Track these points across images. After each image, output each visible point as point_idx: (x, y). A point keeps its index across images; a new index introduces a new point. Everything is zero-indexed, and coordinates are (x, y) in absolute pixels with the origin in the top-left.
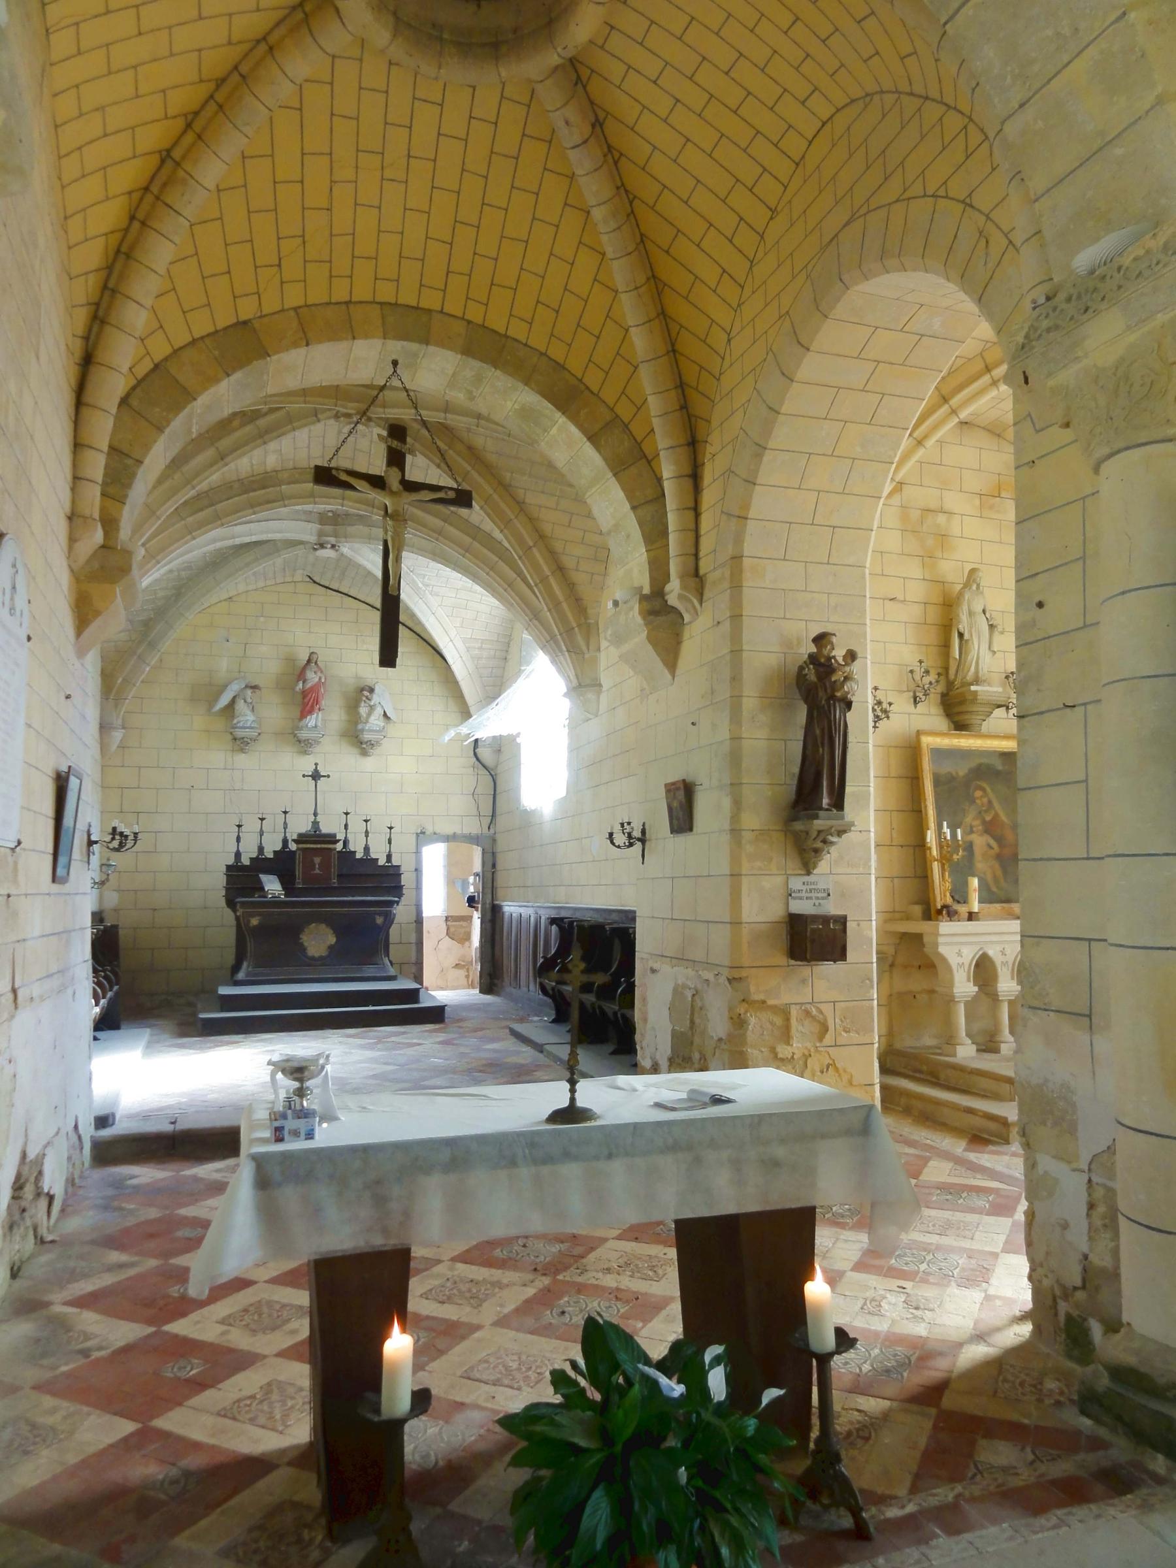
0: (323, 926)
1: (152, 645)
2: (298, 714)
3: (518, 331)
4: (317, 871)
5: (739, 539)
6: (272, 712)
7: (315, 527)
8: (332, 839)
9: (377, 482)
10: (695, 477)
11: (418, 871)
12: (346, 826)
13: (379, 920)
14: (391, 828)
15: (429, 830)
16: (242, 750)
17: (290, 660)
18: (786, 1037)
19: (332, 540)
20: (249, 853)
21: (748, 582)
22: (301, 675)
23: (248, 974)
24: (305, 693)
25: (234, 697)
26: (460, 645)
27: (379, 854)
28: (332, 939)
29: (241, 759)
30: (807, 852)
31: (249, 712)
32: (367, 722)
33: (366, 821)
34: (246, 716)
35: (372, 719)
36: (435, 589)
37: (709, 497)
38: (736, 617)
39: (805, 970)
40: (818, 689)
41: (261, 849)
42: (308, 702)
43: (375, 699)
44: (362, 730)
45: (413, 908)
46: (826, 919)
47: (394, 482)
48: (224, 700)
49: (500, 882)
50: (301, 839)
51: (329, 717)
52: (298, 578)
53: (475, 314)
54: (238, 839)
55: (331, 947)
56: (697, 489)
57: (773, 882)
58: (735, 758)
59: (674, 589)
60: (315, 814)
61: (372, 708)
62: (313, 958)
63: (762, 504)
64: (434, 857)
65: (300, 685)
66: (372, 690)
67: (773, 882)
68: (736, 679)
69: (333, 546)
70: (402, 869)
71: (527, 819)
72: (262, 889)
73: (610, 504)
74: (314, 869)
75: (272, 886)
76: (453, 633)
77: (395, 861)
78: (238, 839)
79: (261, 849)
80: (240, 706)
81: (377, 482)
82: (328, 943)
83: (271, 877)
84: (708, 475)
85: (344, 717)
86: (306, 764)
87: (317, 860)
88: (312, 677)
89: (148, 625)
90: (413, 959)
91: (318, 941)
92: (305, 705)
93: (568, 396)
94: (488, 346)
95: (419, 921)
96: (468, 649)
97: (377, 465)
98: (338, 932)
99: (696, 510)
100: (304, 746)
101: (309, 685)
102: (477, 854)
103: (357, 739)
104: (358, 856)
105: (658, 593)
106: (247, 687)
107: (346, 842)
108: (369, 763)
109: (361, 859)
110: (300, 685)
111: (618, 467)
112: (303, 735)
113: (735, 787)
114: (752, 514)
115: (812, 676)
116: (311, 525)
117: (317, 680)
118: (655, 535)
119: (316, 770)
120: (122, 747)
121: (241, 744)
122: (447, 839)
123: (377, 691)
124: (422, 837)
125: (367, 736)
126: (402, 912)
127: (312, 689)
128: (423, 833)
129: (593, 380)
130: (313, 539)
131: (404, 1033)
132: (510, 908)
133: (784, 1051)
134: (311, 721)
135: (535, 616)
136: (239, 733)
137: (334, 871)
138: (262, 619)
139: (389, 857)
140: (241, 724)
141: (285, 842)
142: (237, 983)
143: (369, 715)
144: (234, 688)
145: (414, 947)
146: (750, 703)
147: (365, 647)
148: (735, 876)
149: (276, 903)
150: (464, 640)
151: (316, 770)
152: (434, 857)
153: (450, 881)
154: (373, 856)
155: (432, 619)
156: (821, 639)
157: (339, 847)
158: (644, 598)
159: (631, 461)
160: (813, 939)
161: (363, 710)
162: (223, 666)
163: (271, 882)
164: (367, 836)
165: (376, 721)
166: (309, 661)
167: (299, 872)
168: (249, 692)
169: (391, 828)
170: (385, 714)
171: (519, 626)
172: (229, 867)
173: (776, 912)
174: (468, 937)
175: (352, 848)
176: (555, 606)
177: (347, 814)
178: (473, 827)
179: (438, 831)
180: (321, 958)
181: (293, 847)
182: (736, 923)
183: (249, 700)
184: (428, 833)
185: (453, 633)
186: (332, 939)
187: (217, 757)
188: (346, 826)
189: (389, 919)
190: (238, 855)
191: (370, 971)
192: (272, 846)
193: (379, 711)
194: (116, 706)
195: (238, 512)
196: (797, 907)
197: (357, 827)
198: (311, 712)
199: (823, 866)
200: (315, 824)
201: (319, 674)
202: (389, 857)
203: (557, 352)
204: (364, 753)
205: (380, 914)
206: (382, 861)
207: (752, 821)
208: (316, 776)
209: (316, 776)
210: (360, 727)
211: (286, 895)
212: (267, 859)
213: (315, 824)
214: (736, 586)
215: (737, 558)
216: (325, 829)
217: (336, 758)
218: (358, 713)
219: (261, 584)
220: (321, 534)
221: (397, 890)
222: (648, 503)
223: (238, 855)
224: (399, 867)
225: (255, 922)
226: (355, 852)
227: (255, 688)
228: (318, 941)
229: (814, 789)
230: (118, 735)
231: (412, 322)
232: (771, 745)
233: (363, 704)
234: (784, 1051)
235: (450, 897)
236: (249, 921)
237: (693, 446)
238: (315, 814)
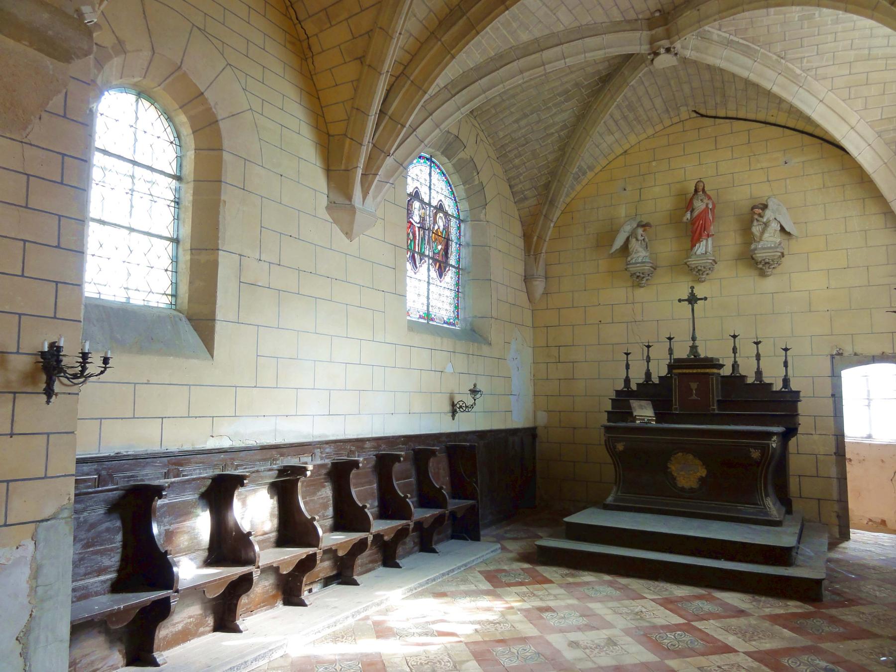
0: (691, 457)
1: (552, 203)
2: (690, 245)
4: (694, 397)
6: (667, 247)
7: (645, 34)
8: (713, 363)
12: (735, 350)
13: (755, 454)
14: (786, 350)
15: (848, 350)
16: (640, 286)
19: (665, 43)
20: (637, 377)
22: (689, 206)
23: (615, 500)
24: (693, 221)
25: (628, 239)
26: (870, 134)
27: (773, 376)
28: (703, 472)
29: (640, 293)
31: (640, 249)
32: (761, 240)
33: (757, 343)
34: (639, 253)
35: (766, 235)
36: (820, 71)
41: (648, 374)
42: (696, 230)
43: (768, 214)
44: (755, 249)
45: (832, 440)
48: (619, 243)
51: (722, 241)
52: (684, 115)
54: (628, 367)
55: (701, 479)
60: (694, 339)
61: (766, 225)
62: (683, 489)
65: (688, 216)
66: (765, 207)
69: (668, 50)
70: (802, 394)
72: (632, 413)
74: (692, 395)
75: (644, 412)
76: (853, 119)
77: (794, 387)
78: (628, 367)
79: (648, 374)
80: (633, 244)
82: (699, 474)
83: (643, 403)
85: (739, 240)
87: (694, 386)
88: (699, 206)
89: (547, 186)
90: (835, 496)
92: (694, 233)
96: (880, 134)
101: (696, 213)
104: (750, 380)
106: (639, 226)
107: (735, 366)
108: (770, 284)
109: (753, 384)
110: (688, 216)
112: (693, 261)
116: (638, 34)
117: (703, 207)
119: (692, 294)
120: (546, 293)
121: (638, 279)
123: (771, 204)
127: (699, 215)
128: (841, 354)
130: (644, 49)
131: (741, 613)
134: (701, 248)
136: (633, 269)
137: (716, 395)
138: (654, 164)
139: (786, 381)
140: (633, 261)
142: (607, 507)
143: (763, 233)
144: (628, 228)
145: (835, 482)
147: (759, 166)
150: (872, 125)
151: (692, 294)
154: (767, 380)
155: (821, 108)
157: (727, 371)
161: (756, 229)
162: (622, 212)
163: (641, 407)
164: (648, 357)
165: (771, 237)
166: (696, 191)
168: (640, 231)
169: (786, 350)
170: (782, 229)
172: (618, 393)
175: (742, 371)
177: (734, 337)
179: (859, 351)
180: (692, 490)
183: (640, 238)
184: (846, 354)
185: (853, 119)
186: (703, 472)
187: (618, 292)
188: (735, 350)
190: (627, 381)
191: (748, 510)
192: (660, 370)
193: (774, 226)
194: (536, 259)
195: (490, 14)
197: (747, 351)
198: (699, 240)
200: (694, 348)
201: (706, 201)
202: (786, 381)
204: (763, 274)
205: (755, 447)
206: (778, 386)
209: (692, 299)
210: (753, 247)
211: (657, 422)
212: (654, 384)
213: (694, 348)
218: (752, 233)
219: (650, 131)
220: (652, 41)
223: (627, 381)
224: (798, 392)
225: (620, 447)
226: (745, 377)
227: (644, 226)
228: (688, 473)
230: (539, 286)
233: (755, 223)
236: (615, 447)
238: (694, 339)
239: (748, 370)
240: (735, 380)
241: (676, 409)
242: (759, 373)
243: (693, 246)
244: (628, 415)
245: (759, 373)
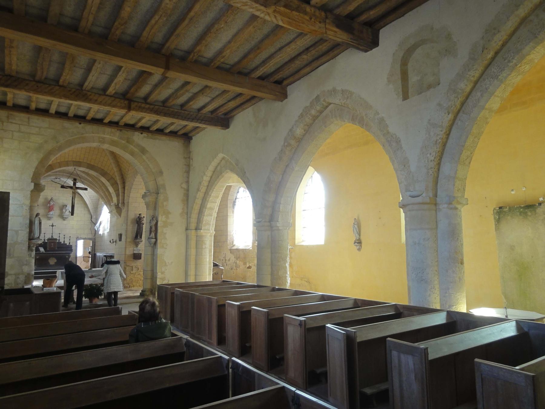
3: (95, 165)
5: (129, 199)
8: (56, 239)
9: (71, 188)
10: (124, 188)
11: (76, 246)
15: (79, 237)
17: (46, 199)
18: (132, 270)
21: (130, 205)
22: (49, 202)
24: (50, 207)
28: (56, 261)
30: (137, 245)
37: (126, 191)
38: (128, 211)
39: (136, 261)
40: (139, 221)
42: (50, 209)
43: (67, 208)
46: (138, 254)
47: (74, 188)
49: (96, 248)
50: (48, 239)
51: (56, 212)
53: (88, 162)
56: (124, 190)
57: (131, 249)
58: (126, 231)
59: (120, 205)
61: (66, 210)
63: (132, 195)
64: (80, 244)
66: (66, 206)
67: (131, 249)
68: (127, 220)
71: (102, 237)
73: (111, 190)
75: (42, 250)
81: (71, 188)
84: (126, 188)
86: (50, 222)
88: (52, 203)
91: (52, 261)
93: (104, 174)
94: (90, 167)
95: (76, 257)
97: (72, 185)
98: (57, 259)
99: (124, 193)
100: (49, 218)
102: (91, 241)
103: (62, 217)
105: (118, 205)
108: (65, 222)
111: (112, 185)
112: (49, 216)
113: (126, 236)
114: (131, 196)
115: (138, 220)
118: (118, 195)
122: (83, 239)
124: (78, 239)
125: (65, 216)
126: (72, 255)
129: (108, 172)
132: (98, 254)
133: (132, 272)
134: (51, 213)
135: (102, 198)
141: (44, 240)
146: (129, 223)
148: (126, 248)
149: (43, 253)
152: (80, 244)
153: (85, 248)
156: (140, 214)
158: (115, 205)
159: (114, 184)
160: (137, 257)
161: (64, 210)
167: (48, 247)
171: (101, 200)
173: (132, 253)
174: (89, 261)
176: (106, 197)
178: (90, 236)
181: (46, 241)
182: (125, 254)
186: (56, 261)
189: (69, 256)
196: (135, 252)
197: (62, 236)
199: (139, 246)
200: (52, 236)
203: (102, 168)
204: (64, 220)
207: (129, 240)
208: (52, 226)
209: (52, 226)
213: (52, 236)
214: (128, 206)
215: (128, 202)
216: (54, 237)
217: (57, 221)
221: (71, 250)
222: (117, 191)
229: (138, 235)
231: (78, 164)
232: (132, 229)
234: (132, 272)
235: (84, 252)
237: (124, 183)
239: (62, 241)
240: (59, 243)
241: (48, 249)
242: (64, 242)
243: (49, 212)
244: (39, 250)
245: (64, 242)
